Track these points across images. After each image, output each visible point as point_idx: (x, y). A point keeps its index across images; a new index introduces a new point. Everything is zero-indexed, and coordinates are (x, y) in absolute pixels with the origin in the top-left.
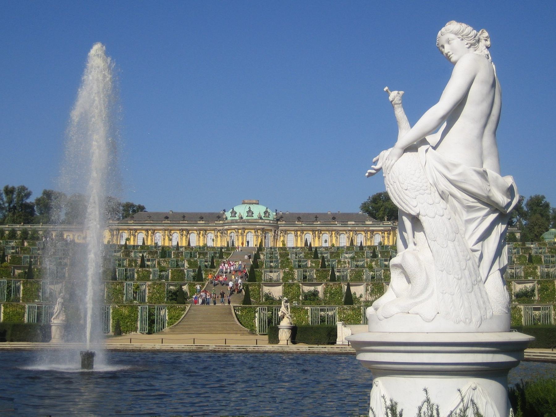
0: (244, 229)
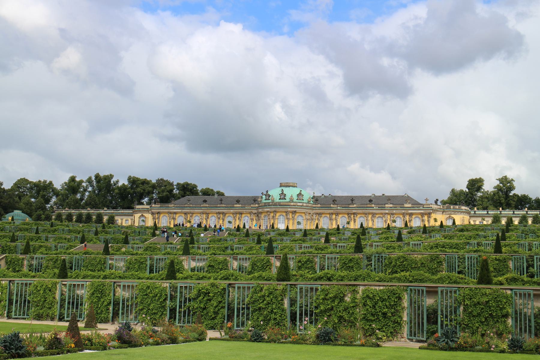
0: (275, 212)
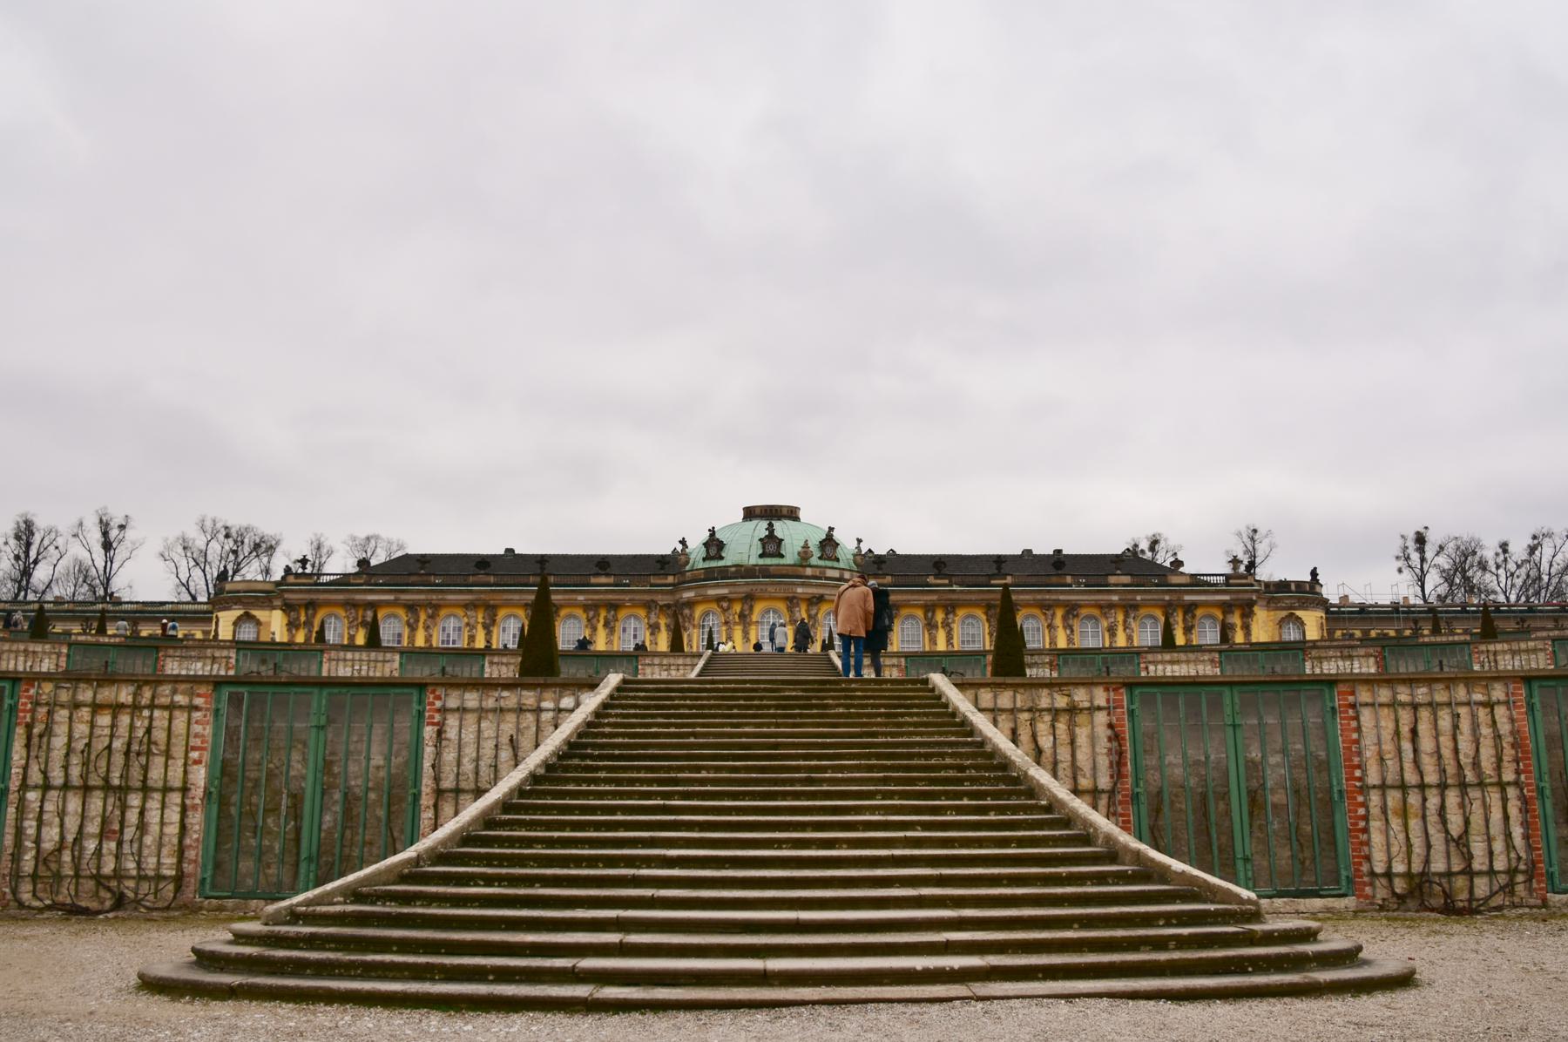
0: (749, 599)
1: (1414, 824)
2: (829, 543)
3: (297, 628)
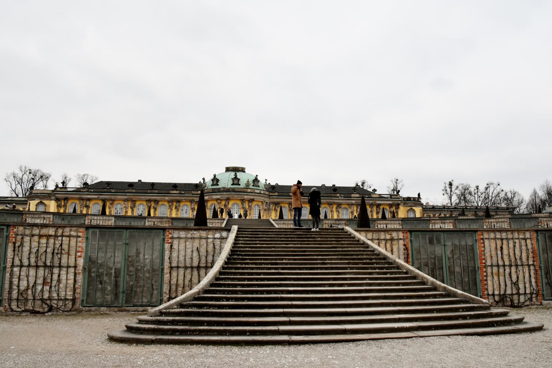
0: (228, 199)
1: (502, 278)
2: (256, 180)
3: (61, 207)
